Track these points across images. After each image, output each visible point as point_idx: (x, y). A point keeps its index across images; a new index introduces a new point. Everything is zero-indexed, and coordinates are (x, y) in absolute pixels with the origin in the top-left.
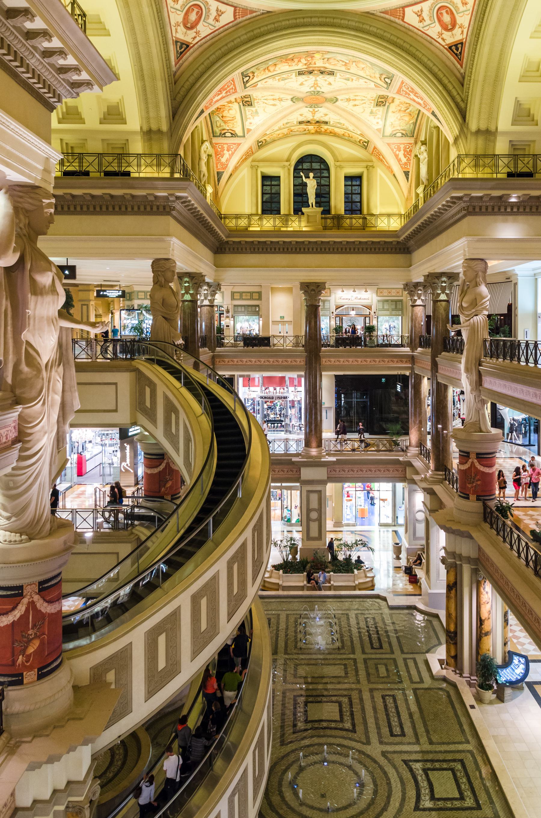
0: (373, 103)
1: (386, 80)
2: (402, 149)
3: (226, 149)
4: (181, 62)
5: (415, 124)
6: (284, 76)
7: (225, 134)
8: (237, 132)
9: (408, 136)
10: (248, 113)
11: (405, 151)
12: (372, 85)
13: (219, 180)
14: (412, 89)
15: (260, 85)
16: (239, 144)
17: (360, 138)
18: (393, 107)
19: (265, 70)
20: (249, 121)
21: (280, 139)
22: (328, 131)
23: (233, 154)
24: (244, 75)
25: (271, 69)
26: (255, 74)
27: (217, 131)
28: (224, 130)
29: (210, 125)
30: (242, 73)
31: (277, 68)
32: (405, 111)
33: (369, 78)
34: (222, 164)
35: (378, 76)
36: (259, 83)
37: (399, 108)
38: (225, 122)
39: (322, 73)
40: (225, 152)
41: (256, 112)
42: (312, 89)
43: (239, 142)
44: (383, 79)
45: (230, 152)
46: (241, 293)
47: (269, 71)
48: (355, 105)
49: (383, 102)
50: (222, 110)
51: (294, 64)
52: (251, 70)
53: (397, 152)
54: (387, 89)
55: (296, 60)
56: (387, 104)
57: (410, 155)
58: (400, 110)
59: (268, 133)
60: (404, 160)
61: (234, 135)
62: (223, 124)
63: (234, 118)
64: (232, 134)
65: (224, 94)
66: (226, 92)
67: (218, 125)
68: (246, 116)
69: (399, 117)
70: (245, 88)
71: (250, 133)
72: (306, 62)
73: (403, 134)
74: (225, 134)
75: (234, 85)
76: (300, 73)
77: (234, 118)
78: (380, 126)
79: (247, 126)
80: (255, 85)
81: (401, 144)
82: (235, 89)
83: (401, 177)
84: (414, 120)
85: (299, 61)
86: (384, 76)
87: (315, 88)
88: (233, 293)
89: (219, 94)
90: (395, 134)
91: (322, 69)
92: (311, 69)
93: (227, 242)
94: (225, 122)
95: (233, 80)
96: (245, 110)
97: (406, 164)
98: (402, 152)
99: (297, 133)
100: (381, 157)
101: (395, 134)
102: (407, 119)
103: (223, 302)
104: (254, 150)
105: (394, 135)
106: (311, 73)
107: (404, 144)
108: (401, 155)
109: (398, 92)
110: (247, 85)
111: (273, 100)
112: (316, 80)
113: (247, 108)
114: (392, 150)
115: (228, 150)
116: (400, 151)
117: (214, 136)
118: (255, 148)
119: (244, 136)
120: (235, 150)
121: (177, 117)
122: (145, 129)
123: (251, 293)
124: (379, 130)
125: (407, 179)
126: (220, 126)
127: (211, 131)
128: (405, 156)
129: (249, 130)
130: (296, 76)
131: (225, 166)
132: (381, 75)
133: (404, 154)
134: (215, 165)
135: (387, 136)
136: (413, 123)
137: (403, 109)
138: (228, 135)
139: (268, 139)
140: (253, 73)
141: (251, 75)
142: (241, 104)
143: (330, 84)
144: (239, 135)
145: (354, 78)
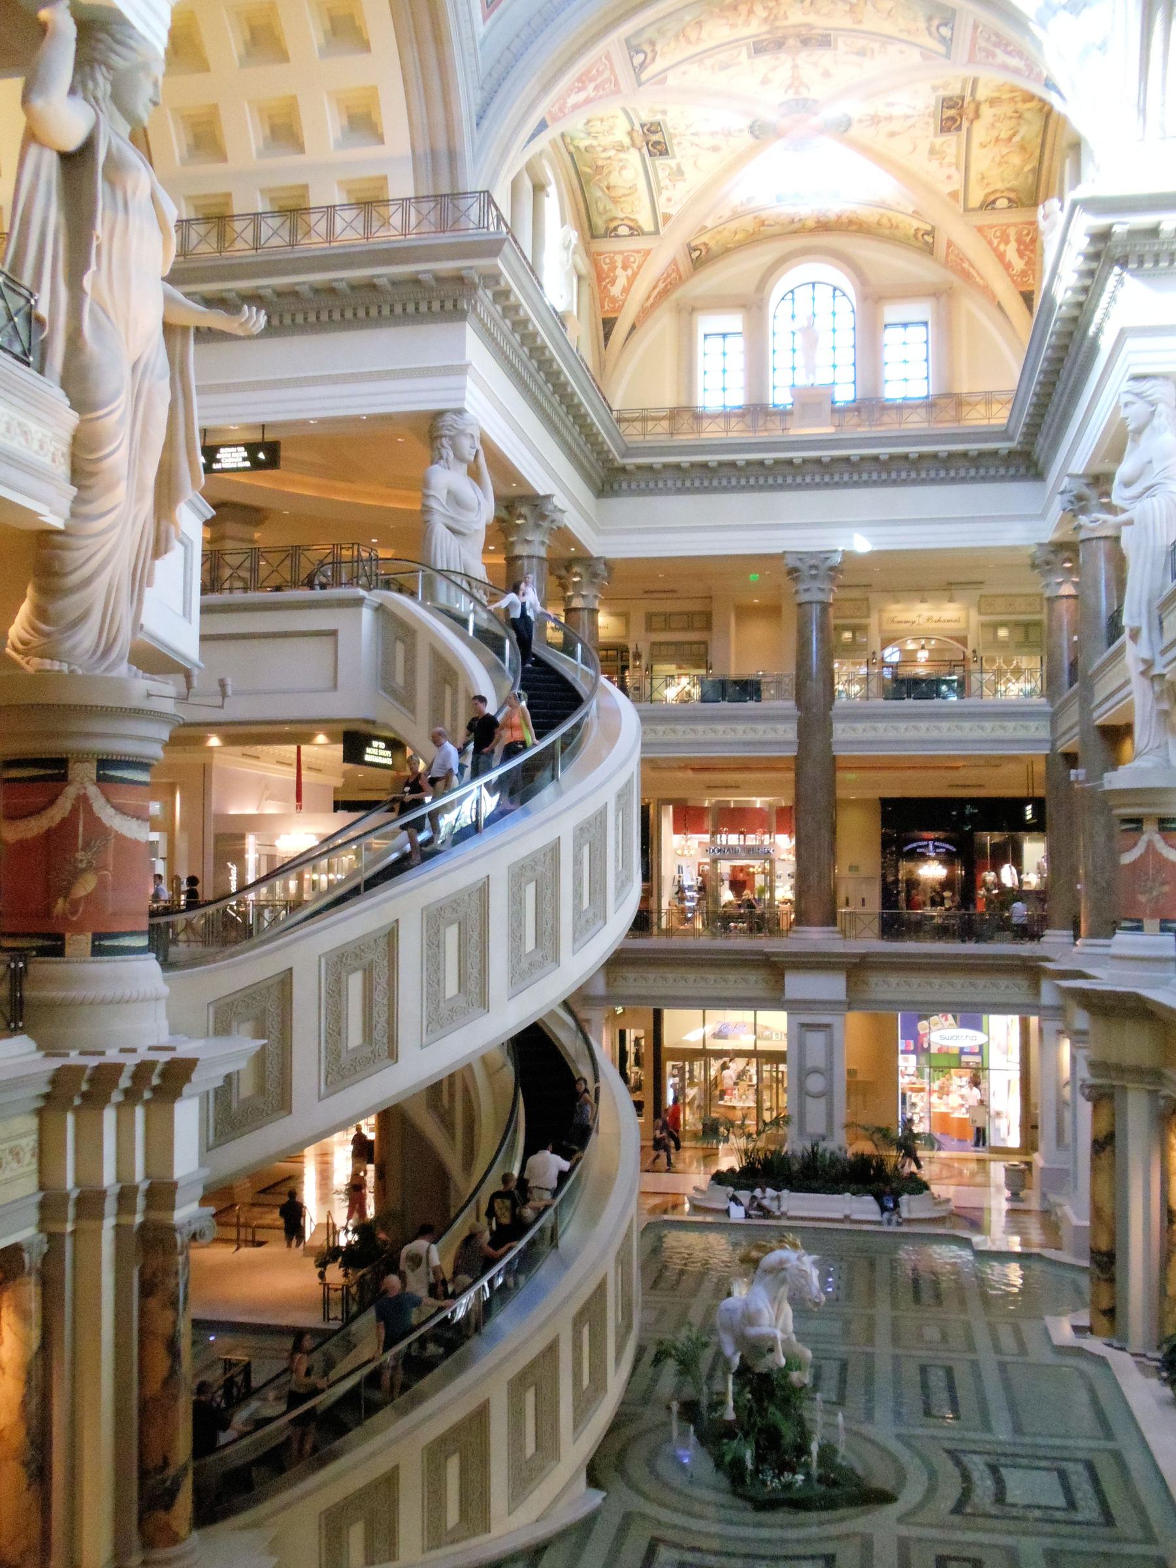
0: (932, 126)
1: (944, 31)
2: (1013, 238)
3: (619, 264)
4: (496, 14)
5: (1037, 171)
6: (723, 57)
7: (615, 229)
9: (1023, 205)
10: (662, 175)
11: (1019, 241)
12: (915, 56)
13: (607, 337)
14: (997, 35)
15: (672, 79)
16: (647, 253)
17: (916, 224)
18: (980, 132)
19: (677, 36)
20: (665, 194)
21: (740, 246)
22: (844, 219)
23: (635, 275)
24: (632, 47)
25: (693, 34)
26: (658, 48)
27: (600, 223)
28: (613, 219)
29: (583, 211)
30: (627, 41)
31: (704, 34)
32: (1010, 139)
33: (904, 36)
34: (613, 300)
35: (922, 24)
36: (670, 74)
37: (995, 133)
39: (805, 42)
40: (619, 271)
41: (680, 172)
42: (791, 95)
44: (934, 29)
45: (630, 272)
46: (667, 617)
47: (689, 42)
48: (892, 134)
49: (953, 119)
50: (605, 171)
51: (740, 21)
52: (649, 34)
53: (1002, 247)
54: (948, 56)
55: (743, 9)
56: (965, 124)
57: (1032, 251)
58: (997, 140)
59: (709, 223)
60: (1019, 264)
61: (636, 231)
63: (633, 189)
64: (631, 228)
65: (590, 90)
66: (596, 88)
67: (601, 208)
68: (658, 182)
69: (998, 159)
70: (640, 84)
71: (669, 224)
72: (765, 14)
73: (1010, 200)
74: (615, 229)
75: (612, 71)
76: (759, 49)
77: (633, 189)
78: (957, 184)
79: (660, 211)
80: (660, 78)
81: (1009, 225)
82: (616, 84)
83: (1014, 305)
84: (1033, 163)
85: (751, 12)
86: (936, 22)
87: (797, 92)
88: (650, 618)
89: (579, 90)
90: (994, 202)
91: (804, 31)
92: (780, 34)
93: (623, 469)
94: (615, 201)
95: (608, 57)
96: (654, 167)
97: (1023, 273)
98: (1013, 245)
99: (777, 229)
100: (966, 265)
101: (994, 202)
102: (1016, 160)
103: (627, 635)
104: (682, 269)
105: (988, 205)
106: (779, 44)
107: (1015, 225)
108: (1011, 252)
109: (971, 60)
110: (644, 76)
111: (713, 134)
112: (795, 67)
113: (660, 162)
114: (990, 243)
115: (625, 268)
116: (1007, 243)
117: (593, 237)
118: (684, 266)
119: (657, 232)
120: (639, 267)
121: (485, 123)
122: (420, 150)
123: (690, 615)
124: (954, 195)
125: (1030, 307)
126: (606, 211)
127: (586, 225)
128: (1021, 254)
129: (667, 218)
130: (749, 57)
132: (930, 19)
133: (1018, 250)
135: (974, 210)
136: (1032, 170)
137: (1004, 135)
138: (623, 230)
139: (712, 244)
140: (652, 43)
141: (648, 49)
142: (645, 150)
143: (827, 74)
145: (876, 46)
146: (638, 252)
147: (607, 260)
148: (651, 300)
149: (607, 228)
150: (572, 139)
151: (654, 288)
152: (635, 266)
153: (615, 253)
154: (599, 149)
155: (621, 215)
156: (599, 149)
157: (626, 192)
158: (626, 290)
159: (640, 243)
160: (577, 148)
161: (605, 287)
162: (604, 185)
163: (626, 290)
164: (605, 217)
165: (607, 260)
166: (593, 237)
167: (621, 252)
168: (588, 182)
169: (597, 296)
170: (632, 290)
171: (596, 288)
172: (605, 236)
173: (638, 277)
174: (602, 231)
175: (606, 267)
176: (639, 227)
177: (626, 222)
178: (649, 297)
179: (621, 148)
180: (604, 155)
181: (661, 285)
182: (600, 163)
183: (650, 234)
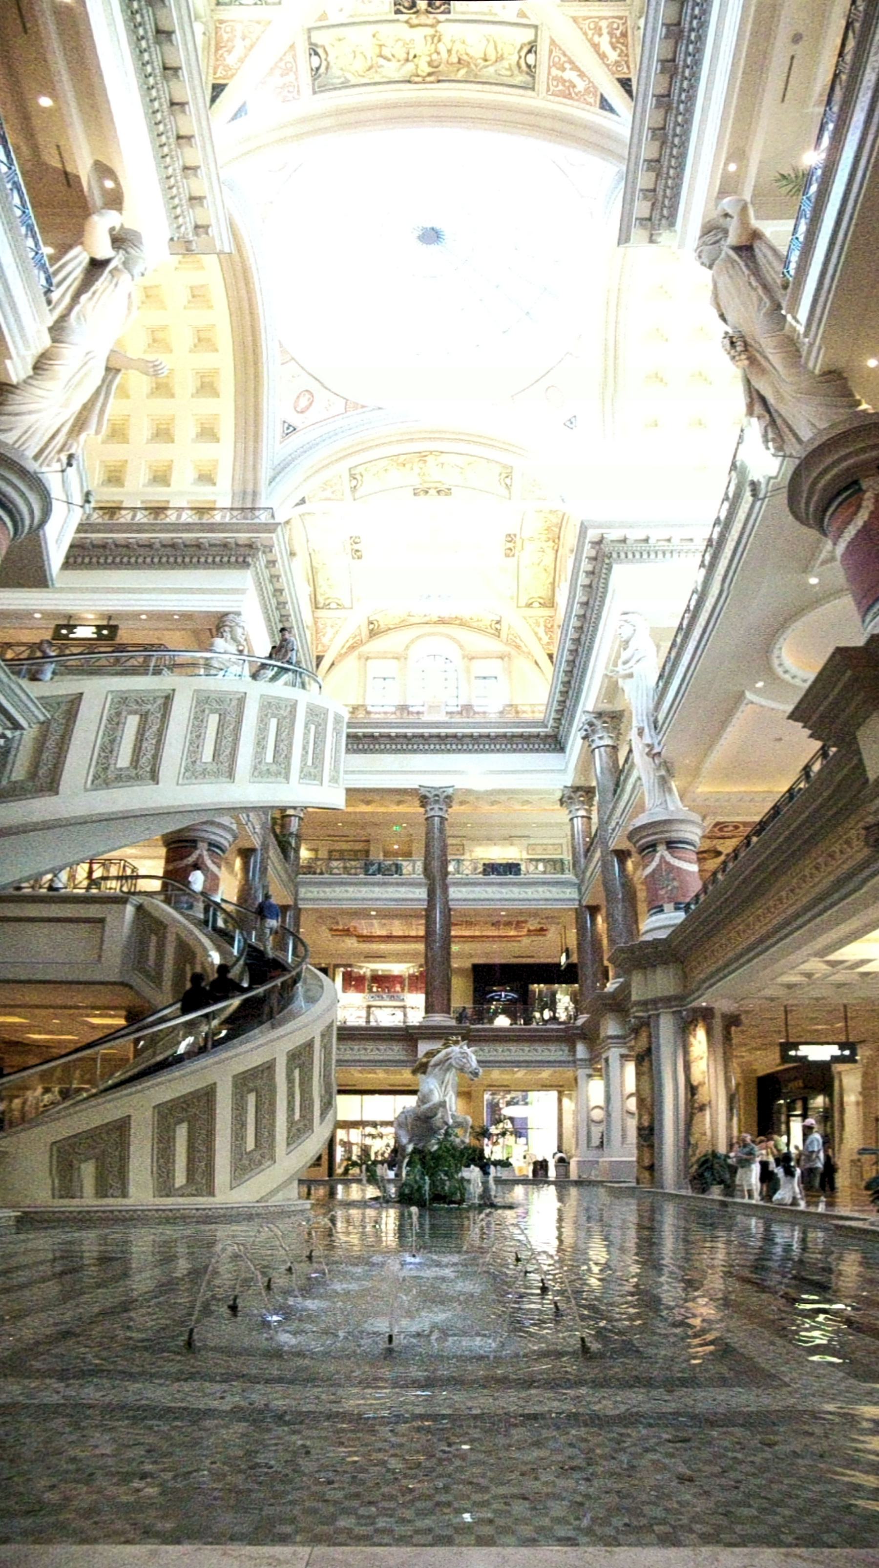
3: (559, 73)
8: (526, 41)
16: (553, 42)
23: (571, 62)
27: (520, 79)
34: (587, 91)
38: (500, 59)
43: (548, 41)
45: (567, 66)
50: (465, 57)
62: (505, 64)
64: (529, 51)
67: (509, 73)
74: (529, 66)
119: (536, 27)
120: (565, 55)
126: (510, 69)
131: (592, 88)
134: (588, 107)
144: (532, 38)
146: (551, 52)
147: (555, 83)
148: (613, 56)
149: (527, 74)
150: (418, 76)
151: (596, 47)
152: (563, 59)
153: (549, 73)
154: (435, 56)
155: (516, 57)
156: (435, 56)
157: (492, 45)
158: (582, 75)
159: (543, 47)
160: (430, 74)
161: (576, 94)
162: (483, 63)
163: (582, 75)
164: (516, 72)
165: (555, 83)
166: (533, 89)
167: (550, 67)
168: (476, 76)
169: (583, 105)
170: (582, 69)
171: (576, 103)
172: (533, 77)
173: (573, 58)
174: (529, 78)
175: (560, 87)
176: (530, 43)
177: (523, 53)
178: (603, 56)
179: (437, 38)
180: (444, 55)
181: (604, 42)
182: (455, 60)
183: (536, 35)
